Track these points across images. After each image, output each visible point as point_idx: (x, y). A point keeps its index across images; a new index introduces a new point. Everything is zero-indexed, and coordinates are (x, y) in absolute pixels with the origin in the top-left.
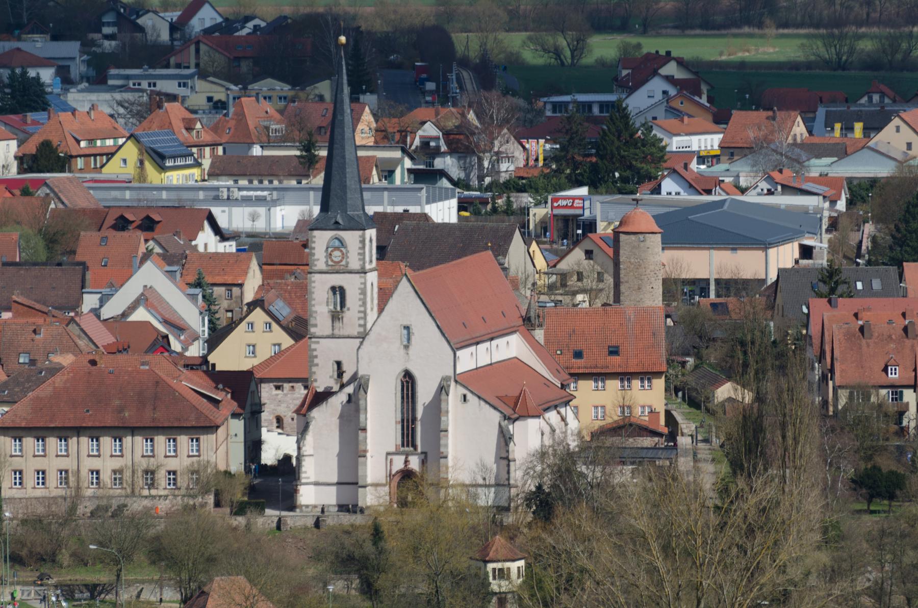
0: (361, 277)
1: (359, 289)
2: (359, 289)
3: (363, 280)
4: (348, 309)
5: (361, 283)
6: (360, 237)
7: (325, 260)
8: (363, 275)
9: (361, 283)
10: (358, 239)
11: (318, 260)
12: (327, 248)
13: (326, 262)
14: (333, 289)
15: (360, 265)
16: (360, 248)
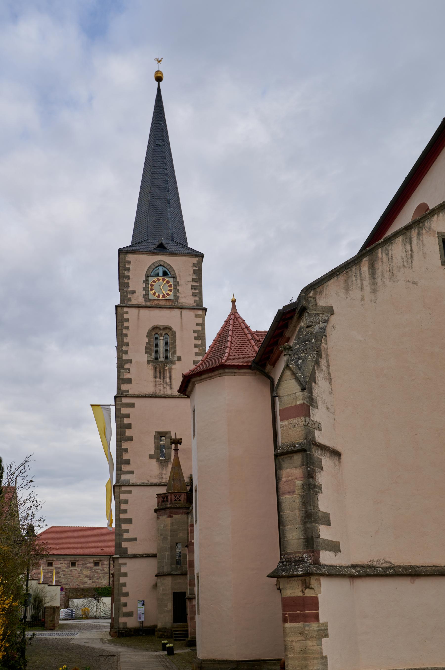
0: (196, 316)
1: (195, 331)
2: (195, 331)
3: (200, 321)
4: (179, 359)
5: (198, 325)
6: (194, 265)
7: (144, 293)
8: (200, 312)
9: (198, 325)
10: (191, 270)
11: (133, 292)
12: (147, 276)
13: (146, 296)
14: (155, 328)
15: (195, 301)
16: (193, 280)
